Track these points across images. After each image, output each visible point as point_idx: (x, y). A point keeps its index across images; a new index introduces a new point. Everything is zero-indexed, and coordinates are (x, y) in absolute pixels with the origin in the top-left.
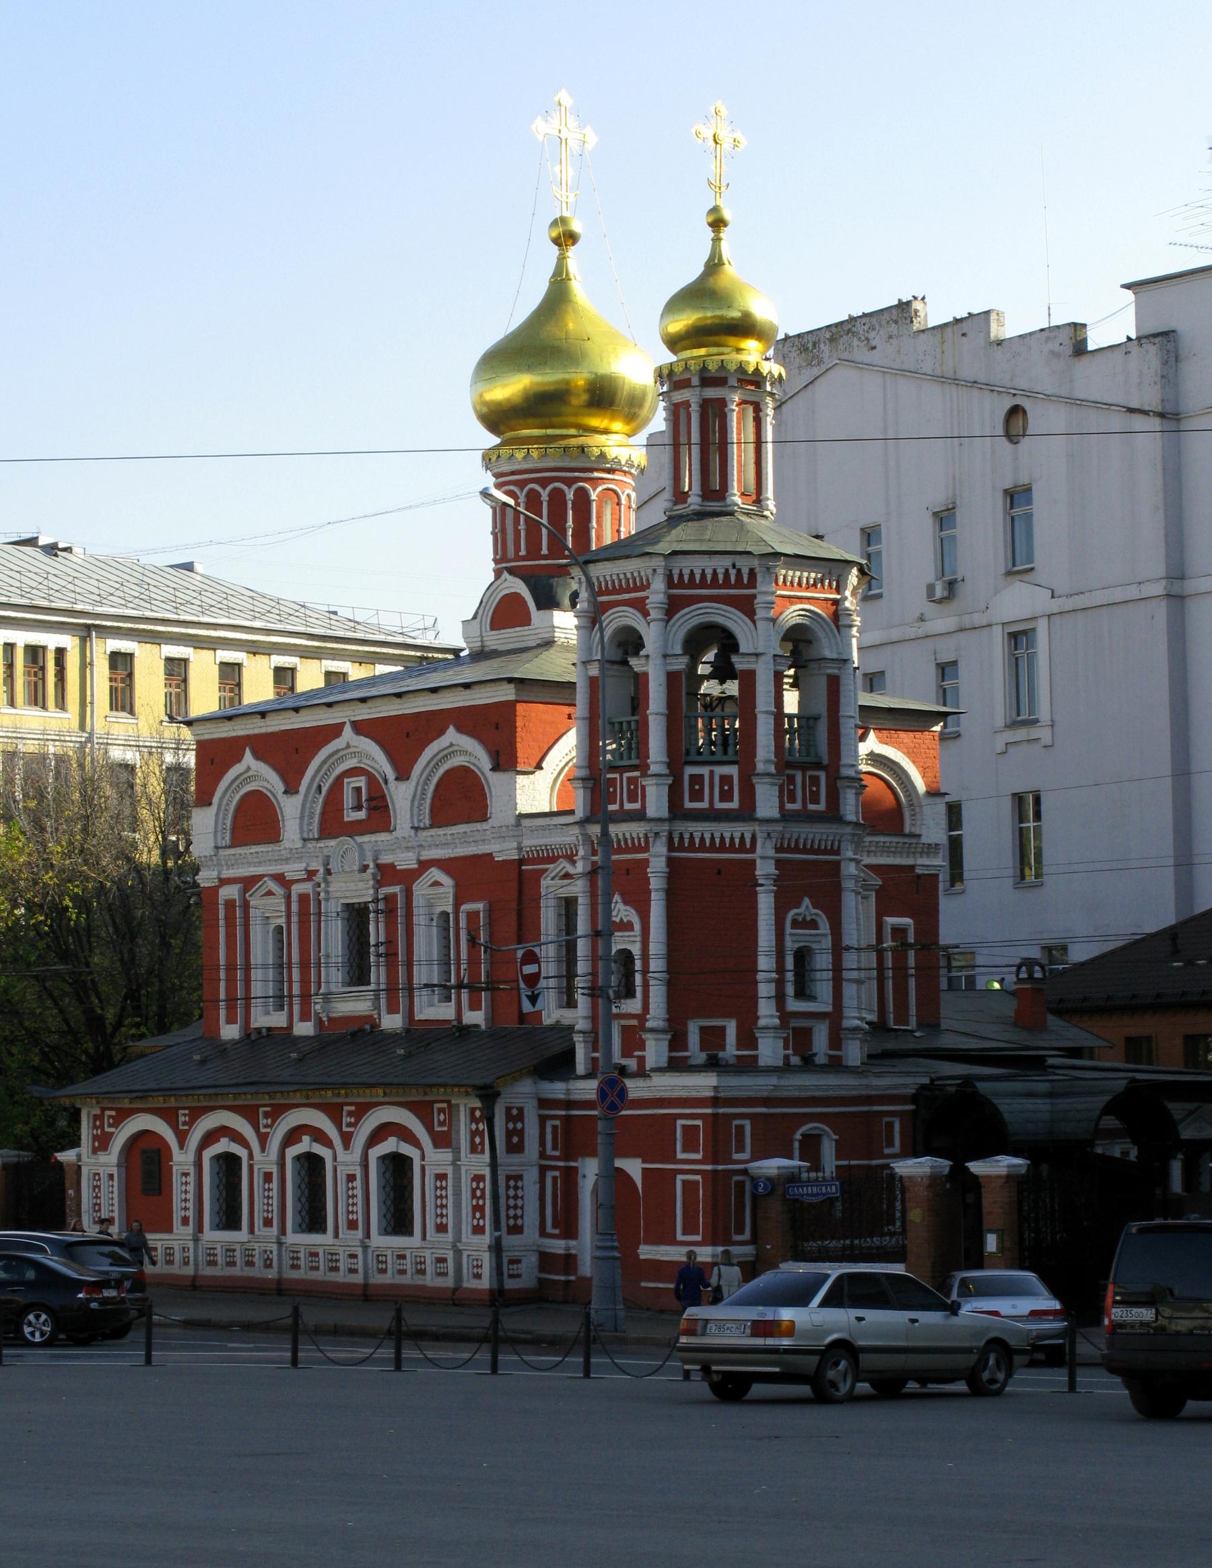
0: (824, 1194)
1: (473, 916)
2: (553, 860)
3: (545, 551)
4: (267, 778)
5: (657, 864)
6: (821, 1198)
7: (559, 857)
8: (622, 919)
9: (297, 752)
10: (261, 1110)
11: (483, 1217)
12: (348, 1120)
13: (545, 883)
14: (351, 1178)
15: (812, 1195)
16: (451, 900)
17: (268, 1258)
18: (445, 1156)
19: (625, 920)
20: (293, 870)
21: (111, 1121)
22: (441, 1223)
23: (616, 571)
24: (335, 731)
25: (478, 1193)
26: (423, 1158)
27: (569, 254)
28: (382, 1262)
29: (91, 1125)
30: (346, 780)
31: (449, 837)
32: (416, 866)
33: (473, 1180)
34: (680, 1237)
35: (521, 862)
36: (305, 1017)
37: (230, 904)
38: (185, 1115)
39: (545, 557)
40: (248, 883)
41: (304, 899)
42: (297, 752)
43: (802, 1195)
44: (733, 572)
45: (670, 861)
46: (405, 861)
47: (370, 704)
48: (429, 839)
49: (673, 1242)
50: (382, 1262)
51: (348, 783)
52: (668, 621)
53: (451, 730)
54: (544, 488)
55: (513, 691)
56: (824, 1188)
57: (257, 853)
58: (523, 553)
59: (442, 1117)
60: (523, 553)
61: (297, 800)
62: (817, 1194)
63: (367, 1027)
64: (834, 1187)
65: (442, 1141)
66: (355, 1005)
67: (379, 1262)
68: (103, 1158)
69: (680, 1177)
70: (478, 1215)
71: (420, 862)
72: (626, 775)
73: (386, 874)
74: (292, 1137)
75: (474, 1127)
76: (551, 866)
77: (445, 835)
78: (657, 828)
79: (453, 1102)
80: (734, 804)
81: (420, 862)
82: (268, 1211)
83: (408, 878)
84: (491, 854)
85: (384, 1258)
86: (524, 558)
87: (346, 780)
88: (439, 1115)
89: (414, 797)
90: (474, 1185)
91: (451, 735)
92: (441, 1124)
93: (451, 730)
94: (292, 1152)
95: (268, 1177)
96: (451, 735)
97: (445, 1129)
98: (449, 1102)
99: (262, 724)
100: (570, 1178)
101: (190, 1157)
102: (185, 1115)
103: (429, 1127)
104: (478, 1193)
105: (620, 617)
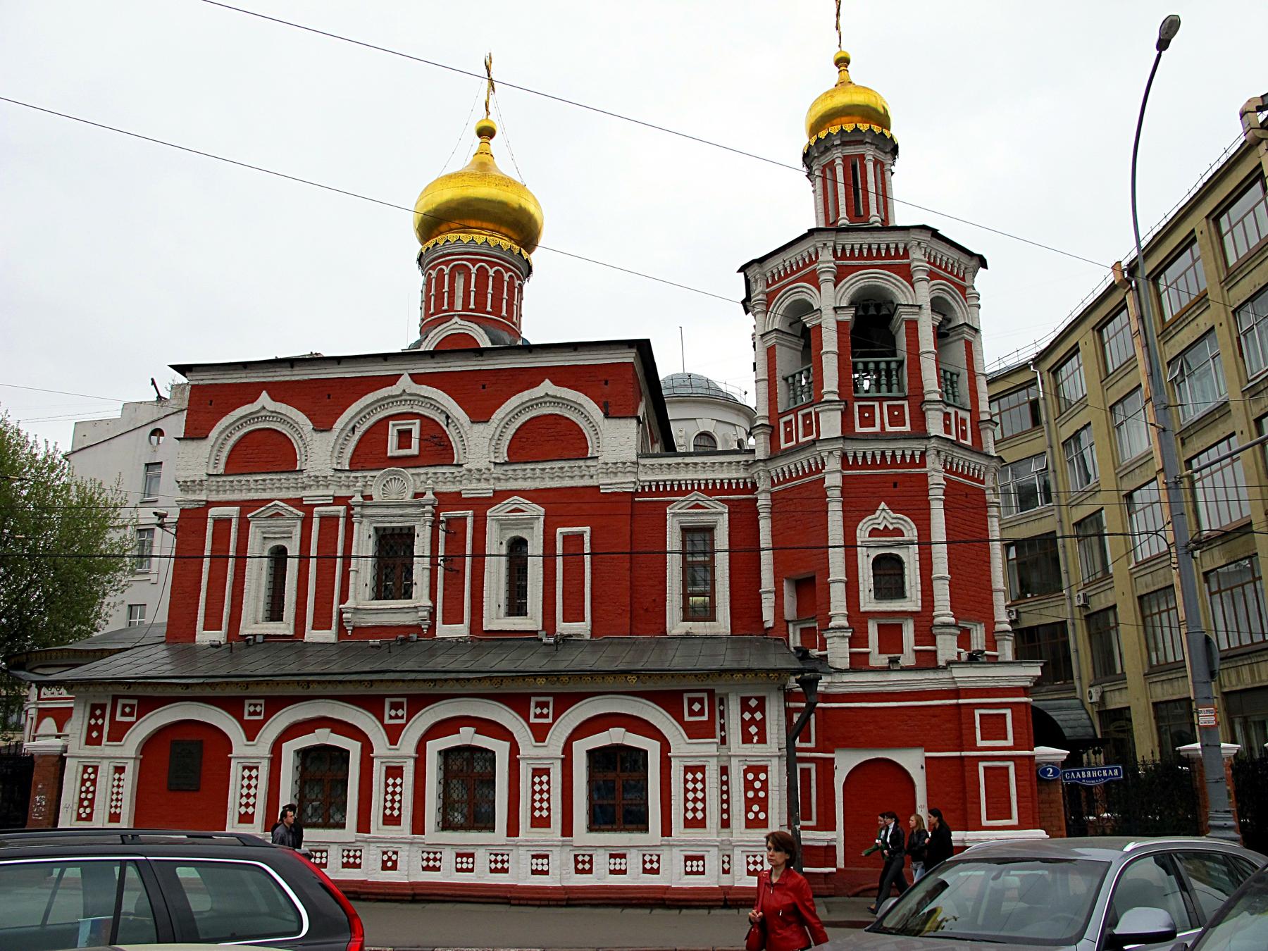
0: (1105, 778)
1: (573, 541)
3: (489, 309)
5: (937, 480)
6: (1102, 781)
8: (886, 525)
11: (764, 808)
12: (538, 711)
14: (537, 772)
15: (1092, 778)
16: (539, 526)
17: (390, 859)
18: (705, 749)
19: (891, 527)
20: (309, 495)
21: (127, 710)
22: (695, 817)
23: (870, 240)
24: (392, 380)
25: (757, 785)
26: (665, 747)
28: (584, 862)
29: (87, 714)
30: (391, 423)
31: (538, 471)
32: (491, 495)
33: (746, 772)
34: (985, 822)
35: (636, 494)
36: (322, 622)
37: (222, 525)
39: (488, 313)
41: (329, 523)
42: (329, 398)
43: (1080, 780)
45: (945, 479)
46: (471, 489)
48: (510, 473)
49: (980, 828)
50: (584, 862)
51: (394, 425)
55: (634, 355)
56: (1104, 772)
57: (264, 480)
58: (472, 306)
59: (696, 707)
60: (472, 306)
61: (330, 437)
62: (1098, 778)
63: (415, 636)
64: (1116, 772)
65: (695, 731)
66: (394, 612)
67: (577, 862)
68: (107, 749)
69: (982, 765)
70: (756, 808)
71: (495, 491)
72: (885, 404)
75: (747, 716)
76: (682, 498)
77: (533, 469)
78: (941, 447)
79: (716, 692)
80: (969, 442)
81: (495, 491)
82: (247, 805)
83: (481, 505)
84: (598, 487)
85: (587, 859)
86: (472, 310)
87: (391, 423)
88: (690, 705)
89: (493, 435)
90: (750, 776)
91: (547, 387)
92: (692, 713)
94: (434, 747)
95: (394, 772)
97: (705, 718)
98: (711, 693)
100: (827, 768)
101: (263, 745)
103: (679, 717)
104: (757, 785)
105: (876, 278)
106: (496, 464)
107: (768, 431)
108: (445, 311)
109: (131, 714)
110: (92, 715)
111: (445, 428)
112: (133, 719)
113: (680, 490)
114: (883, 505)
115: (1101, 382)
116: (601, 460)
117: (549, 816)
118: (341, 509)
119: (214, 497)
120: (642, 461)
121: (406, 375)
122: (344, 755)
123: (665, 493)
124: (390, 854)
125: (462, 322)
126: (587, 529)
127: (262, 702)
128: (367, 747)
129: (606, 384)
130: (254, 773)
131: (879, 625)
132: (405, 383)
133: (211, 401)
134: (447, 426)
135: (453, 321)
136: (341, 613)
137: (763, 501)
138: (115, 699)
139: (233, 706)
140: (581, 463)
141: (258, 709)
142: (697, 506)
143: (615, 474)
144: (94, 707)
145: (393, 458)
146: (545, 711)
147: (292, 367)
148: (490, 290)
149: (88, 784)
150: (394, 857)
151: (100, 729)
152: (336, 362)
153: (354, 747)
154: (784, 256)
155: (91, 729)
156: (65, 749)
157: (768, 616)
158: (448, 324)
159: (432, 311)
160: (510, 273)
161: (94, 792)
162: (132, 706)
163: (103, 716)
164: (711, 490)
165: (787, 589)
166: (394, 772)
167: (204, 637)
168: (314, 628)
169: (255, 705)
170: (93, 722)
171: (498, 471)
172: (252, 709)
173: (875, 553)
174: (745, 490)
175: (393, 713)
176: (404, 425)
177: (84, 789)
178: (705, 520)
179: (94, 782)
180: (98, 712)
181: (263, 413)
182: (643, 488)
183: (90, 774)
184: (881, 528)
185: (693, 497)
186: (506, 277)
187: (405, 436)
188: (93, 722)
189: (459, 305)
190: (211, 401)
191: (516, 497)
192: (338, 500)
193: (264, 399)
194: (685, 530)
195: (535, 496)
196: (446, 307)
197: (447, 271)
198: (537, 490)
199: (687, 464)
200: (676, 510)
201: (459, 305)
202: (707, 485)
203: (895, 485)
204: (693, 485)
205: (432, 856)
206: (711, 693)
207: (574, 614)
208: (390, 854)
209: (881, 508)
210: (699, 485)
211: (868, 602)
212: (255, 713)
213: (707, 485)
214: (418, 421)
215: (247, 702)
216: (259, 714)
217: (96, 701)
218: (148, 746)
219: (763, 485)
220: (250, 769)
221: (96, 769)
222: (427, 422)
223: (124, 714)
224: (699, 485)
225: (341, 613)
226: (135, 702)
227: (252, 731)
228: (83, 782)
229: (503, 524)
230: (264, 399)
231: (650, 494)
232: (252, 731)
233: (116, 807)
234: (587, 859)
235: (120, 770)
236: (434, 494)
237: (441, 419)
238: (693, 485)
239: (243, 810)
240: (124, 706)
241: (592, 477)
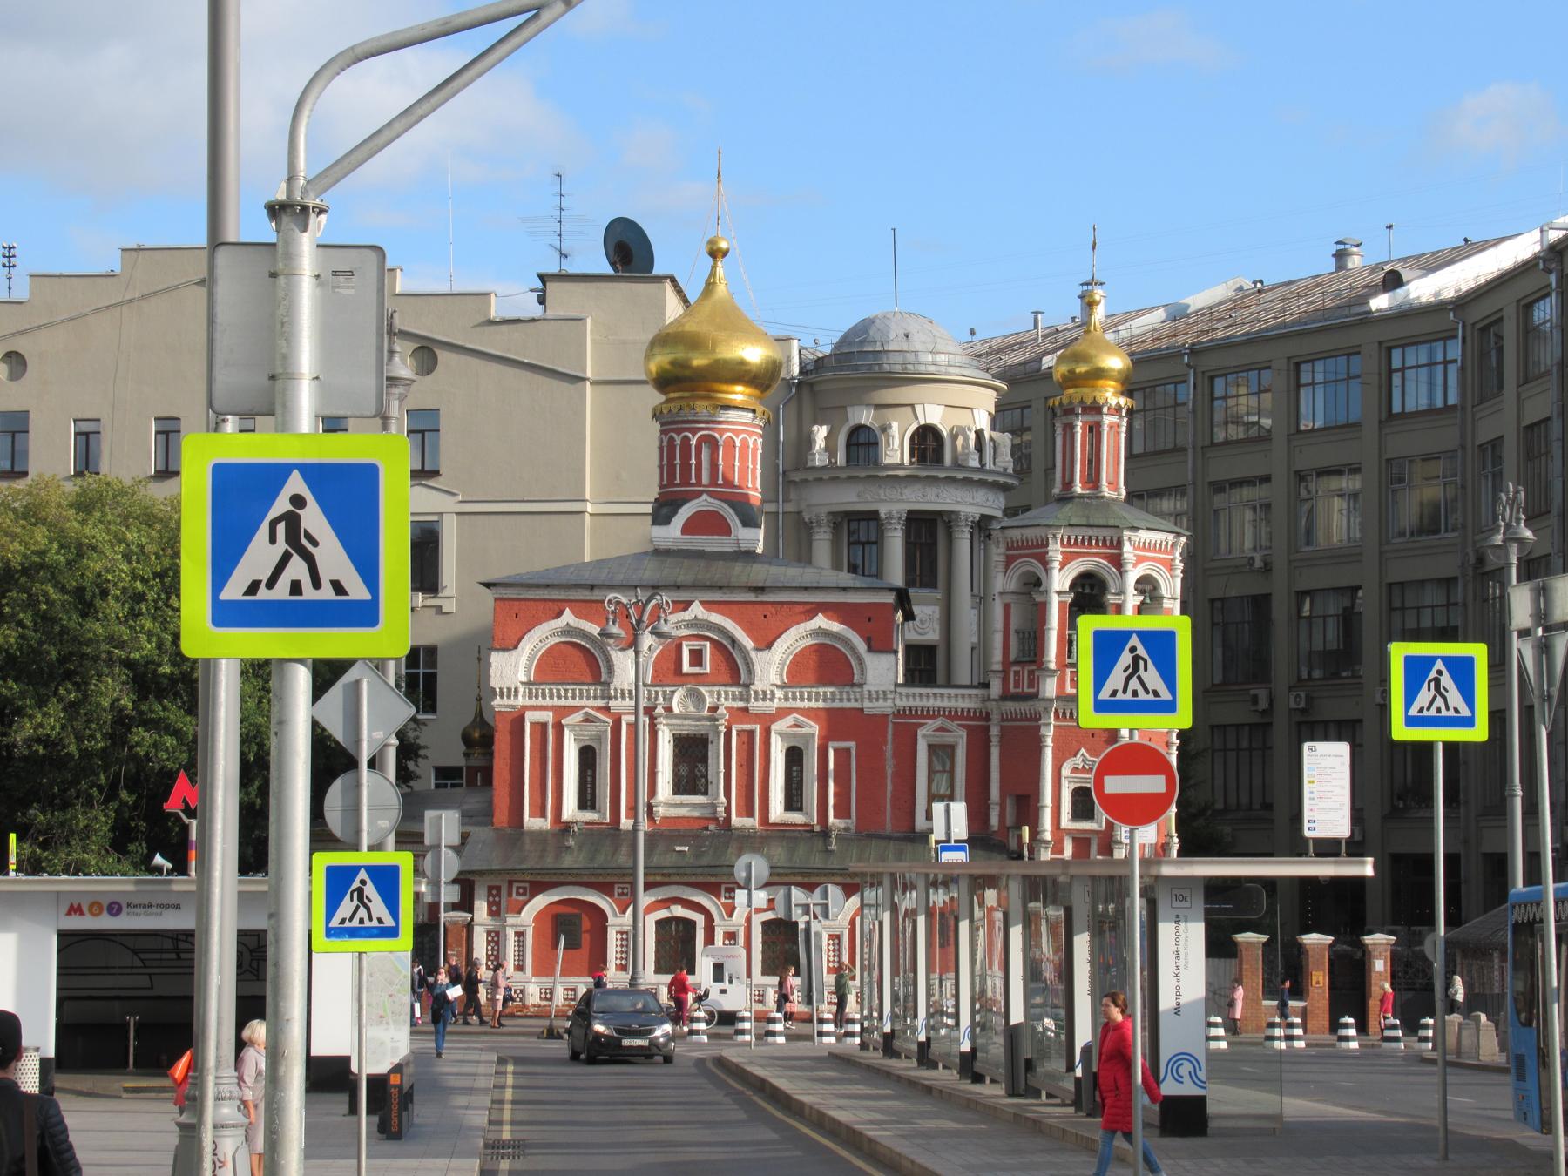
1: (842, 755)
2: (933, 717)
7: (939, 715)
10: (723, 887)
13: (920, 732)
21: (521, 891)
23: (1090, 533)
27: (719, 264)
37: (541, 727)
38: (623, 888)
44: (1164, 543)
46: (756, 706)
47: (725, 590)
54: (738, 437)
58: (720, 481)
68: (511, 920)
76: (930, 722)
83: (767, 720)
84: (862, 710)
106: (777, 686)
107: (1001, 675)
108: (693, 485)
110: (490, 894)
111: (732, 650)
113: (929, 714)
114: (1083, 751)
115: (1519, 386)
116: (866, 687)
119: (528, 702)
120: (899, 690)
121: (697, 602)
122: (691, 925)
123: (916, 717)
125: (712, 500)
126: (852, 745)
128: (709, 919)
129: (870, 620)
131: (1075, 840)
134: (733, 647)
136: (650, 807)
137: (994, 731)
138: (510, 883)
139: (605, 888)
140: (847, 689)
141: (625, 891)
142: (941, 729)
143: (877, 699)
144: (490, 888)
145: (687, 675)
148: (737, 464)
151: (498, 904)
153: (699, 919)
154: (1022, 531)
156: (472, 919)
157: (994, 821)
158: (697, 501)
159: (678, 481)
160: (754, 437)
161: (498, 950)
162: (525, 889)
163: (499, 894)
164: (953, 715)
165: (1009, 802)
167: (531, 822)
169: (623, 888)
171: (779, 693)
172: (620, 891)
173: (1073, 786)
174: (981, 718)
175: (727, 895)
176: (696, 644)
177: (490, 948)
178: (947, 738)
180: (494, 892)
182: (899, 711)
184: (1080, 767)
185: (938, 723)
186: (751, 441)
188: (491, 899)
189: (705, 479)
191: (795, 715)
193: (568, 617)
194: (930, 746)
196: (693, 480)
197: (693, 442)
198: (810, 709)
199: (935, 695)
200: (924, 732)
201: (705, 479)
202: (950, 711)
203: (1093, 735)
204: (939, 711)
209: (1081, 753)
210: (944, 711)
211: (1066, 821)
212: (623, 894)
213: (950, 711)
214: (708, 643)
215: (616, 886)
216: (627, 894)
218: (539, 918)
219: (995, 717)
220: (622, 933)
221: (497, 934)
223: (518, 894)
224: (944, 711)
225: (650, 807)
226: (527, 885)
228: (488, 943)
229: (783, 735)
230: (568, 617)
236: (726, 708)
237: (727, 643)
238: (939, 711)
240: (518, 888)
241: (856, 700)
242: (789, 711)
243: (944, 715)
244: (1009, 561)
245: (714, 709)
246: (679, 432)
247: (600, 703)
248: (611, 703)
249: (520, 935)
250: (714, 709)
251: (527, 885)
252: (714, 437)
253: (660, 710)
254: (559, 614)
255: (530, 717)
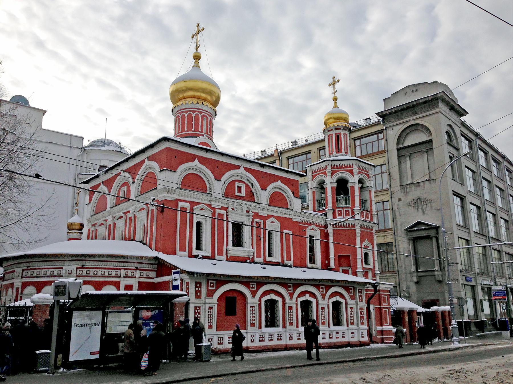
2: (310, 225)
4: (207, 173)
9: (217, 168)
20: (214, 205)
21: (212, 285)
30: (236, 183)
40: (193, 204)
42: (217, 168)
47: (252, 164)
52: (331, 176)
53: (279, 181)
70: (362, 319)
73: (256, 215)
74: (313, 295)
83: (265, 218)
84: (292, 219)
91: (279, 183)
93: (279, 181)
96: (279, 183)
98: (353, 287)
99: (205, 154)
102: (253, 285)
109: (213, 287)
110: (196, 287)
112: (214, 288)
117: (325, 322)
118: (224, 212)
124: (291, 335)
127: (255, 283)
130: (254, 309)
132: (242, 169)
133: (176, 157)
135: (204, 137)
144: (196, 283)
145: (237, 196)
146: (323, 290)
147: (207, 152)
149: (198, 314)
150: (292, 336)
151: (200, 292)
152: (235, 159)
154: (340, 162)
155: (196, 292)
162: (213, 283)
163: (200, 286)
166: (290, 308)
168: (218, 255)
169: (253, 285)
170: (197, 289)
176: (240, 184)
179: (199, 313)
181: (196, 167)
183: (198, 310)
185: (313, 227)
187: (239, 188)
188: (197, 289)
190: (176, 157)
192: (223, 208)
195: (277, 218)
196: (200, 130)
197: (200, 116)
205: (299, 335)
206: (353, 287)
207: (289, 258)
208: (291, 335)
212: (252, 288)
214: (244, 184)
216: (254, 288)
217: (197, 281)
218: (219, 299)
221: (200, 308)
222: (247, 185)
223: (211, 286)
226: (215, 282)
227: (254, 294)
231: (302, 223)
232: (254, 294)
233: (210, 322)
234: (331, 334)
235: (211, 308)
237: (250, 185)
239: (252, 322)
242: (272, 216)
243: (315, 225)
244: (313, 177)
245: (248, 212)
246: (194, 112)
247: (209, 203)
248: (212, 203)
249: (211, 308)
250: (248, 212)
251: (215, 282)
252: (207, 116)
253: (230, 209)
254: (193, 160)
255: (181, 204)
